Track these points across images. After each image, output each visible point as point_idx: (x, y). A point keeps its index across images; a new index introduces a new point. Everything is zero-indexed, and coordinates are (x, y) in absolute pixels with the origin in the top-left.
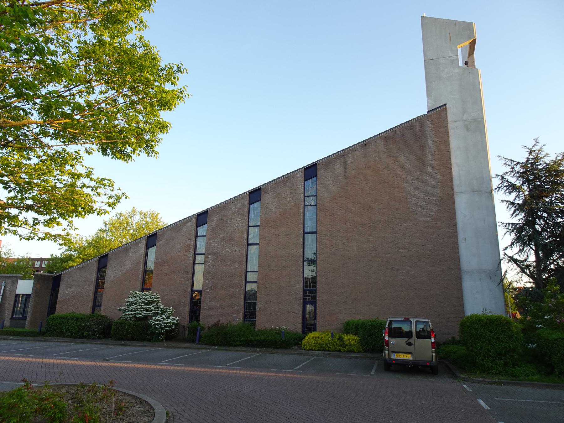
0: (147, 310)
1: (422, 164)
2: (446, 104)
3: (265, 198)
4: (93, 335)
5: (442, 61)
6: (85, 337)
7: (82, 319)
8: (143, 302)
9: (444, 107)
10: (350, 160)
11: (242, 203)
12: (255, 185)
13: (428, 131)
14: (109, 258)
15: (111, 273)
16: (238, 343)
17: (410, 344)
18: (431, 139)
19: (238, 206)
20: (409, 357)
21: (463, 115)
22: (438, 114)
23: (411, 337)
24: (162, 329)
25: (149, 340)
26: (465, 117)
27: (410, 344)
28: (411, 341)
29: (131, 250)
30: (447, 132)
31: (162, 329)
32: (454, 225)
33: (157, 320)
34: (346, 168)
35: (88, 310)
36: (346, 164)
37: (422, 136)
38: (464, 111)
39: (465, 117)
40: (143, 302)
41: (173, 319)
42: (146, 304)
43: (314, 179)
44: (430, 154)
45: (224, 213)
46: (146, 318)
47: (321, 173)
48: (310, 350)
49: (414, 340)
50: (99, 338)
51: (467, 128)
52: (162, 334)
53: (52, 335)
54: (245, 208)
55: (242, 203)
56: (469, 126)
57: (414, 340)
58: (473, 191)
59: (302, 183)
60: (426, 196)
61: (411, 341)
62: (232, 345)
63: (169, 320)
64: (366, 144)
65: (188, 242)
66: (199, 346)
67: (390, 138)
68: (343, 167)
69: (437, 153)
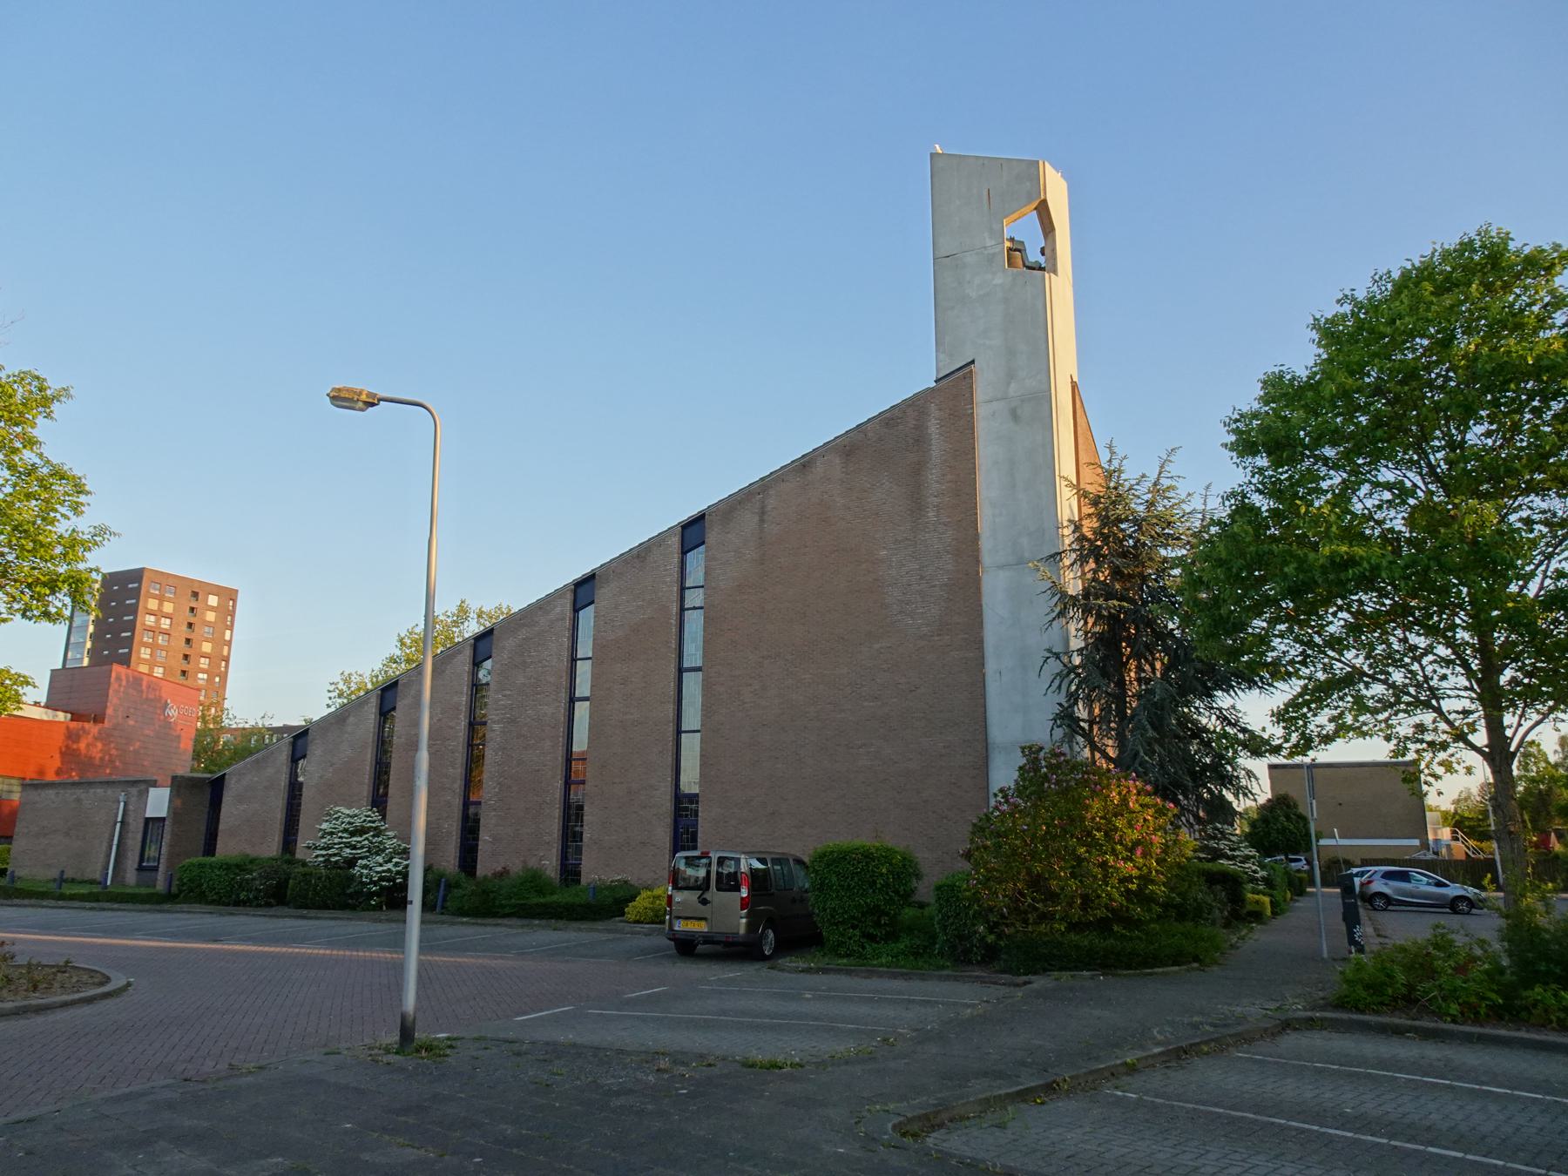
0: (354, 848)
1: (917, 504)
2: (973, 362)
3: (604, 594)
4: (256, 898)
5: (970, 259)
6: (238, 903)
7: (237, 866)
8: (345, 830)
9: (966, 370)
10: (771, 503)
11: (558, 610)
12: (586, 570)
13: (933, 428)
14: (310, 737)
15: (309, 772)
16: (507, 911)
17: (704, 902)
18: (937, 446)
19: (552, 616)
20: (702, 927)
21: (1009, 384)
22: (956, 385)
23: (708, 888)
24: (375, 883)
25: (353, 908)
26: (1013, 389)
27: (704, 902)
28: (708, 896)
29: (351, 719)
30: (971, 428)
31: (375, 883)
32: (977, 644)
33: (365, 867)
34: (762, 521)
35: (271, 847)
36: (763, 513)
37: (920, 440)
38: (1011, 376)
39: (1013, 389)
40: (345, 830)
41: (397, 864)
42: (352, 834)
43: (702, 548)
44: (934, 479)
45: (523, 633)
46: (351, 862)
47: (712, 537)
48: (638, 922)
49: (713, 894)
50: (269, 905)
51: (1014, 415)
52: (374, 894)
53: (187, 900)
54: (563, 619)
55: (558, 610)
56: (1019, 412)
57: (713, 894)
58: (1021, 562)
59: (676, 559)
60: (922, 578)
61: (708, 896)
62: (495, 915)
63: (390, 866)
64: (804, 464)
65: (456, 699)
66: (444, 917)
67: (849, 447)
68: (756, 519)
69: (949, 477)
